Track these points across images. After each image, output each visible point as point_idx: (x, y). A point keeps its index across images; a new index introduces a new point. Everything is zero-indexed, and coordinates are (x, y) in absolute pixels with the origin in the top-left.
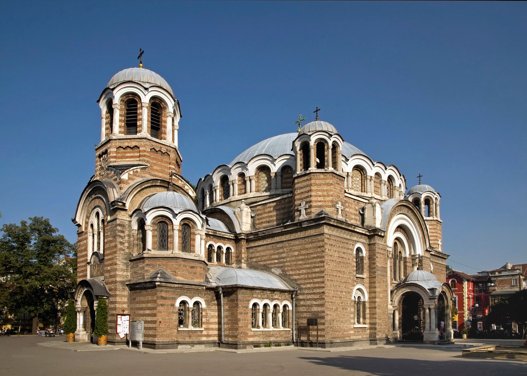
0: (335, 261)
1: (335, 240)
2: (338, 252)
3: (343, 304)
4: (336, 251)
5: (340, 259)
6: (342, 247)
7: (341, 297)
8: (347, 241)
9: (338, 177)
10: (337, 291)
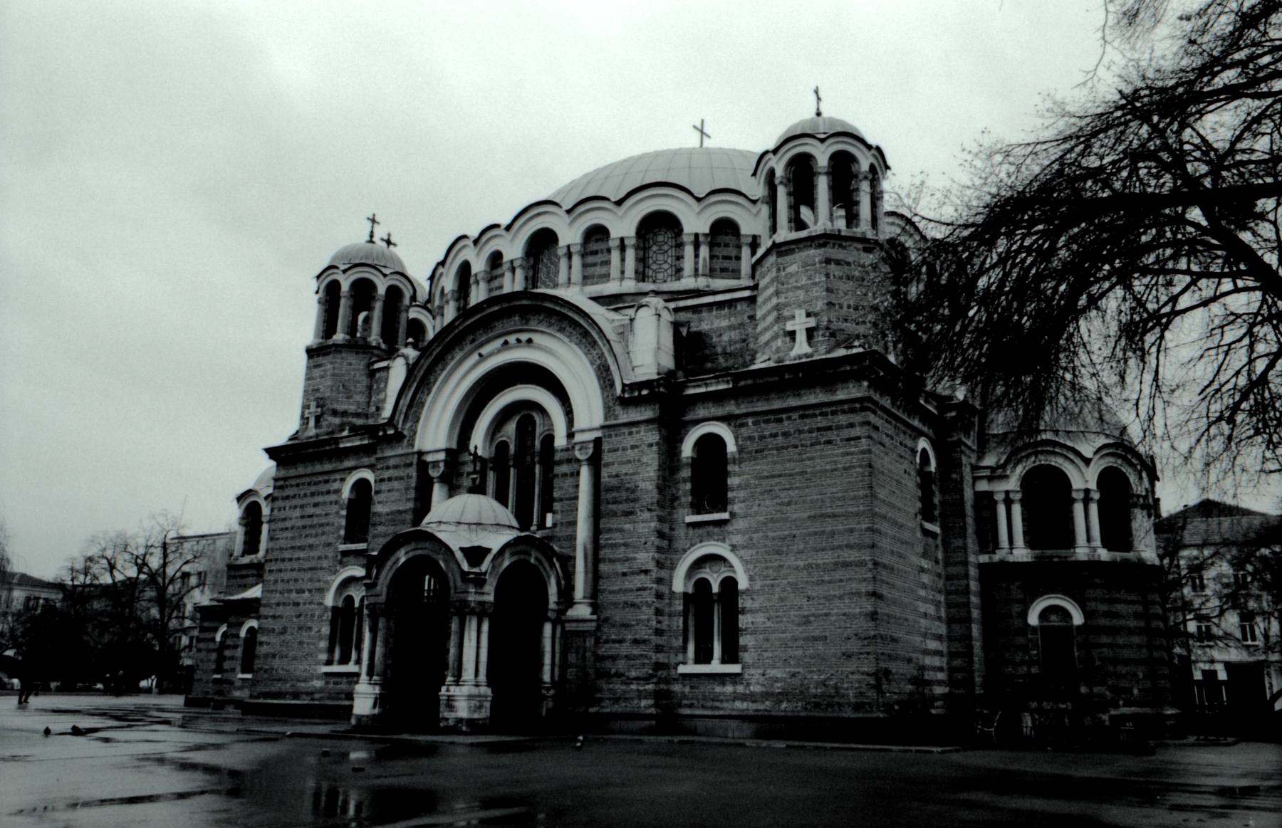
0: (292, 528)
1: (298, 485)
4: (295, 507)
5: (307, 522)
7: (297, 604)
8: (326, 477)
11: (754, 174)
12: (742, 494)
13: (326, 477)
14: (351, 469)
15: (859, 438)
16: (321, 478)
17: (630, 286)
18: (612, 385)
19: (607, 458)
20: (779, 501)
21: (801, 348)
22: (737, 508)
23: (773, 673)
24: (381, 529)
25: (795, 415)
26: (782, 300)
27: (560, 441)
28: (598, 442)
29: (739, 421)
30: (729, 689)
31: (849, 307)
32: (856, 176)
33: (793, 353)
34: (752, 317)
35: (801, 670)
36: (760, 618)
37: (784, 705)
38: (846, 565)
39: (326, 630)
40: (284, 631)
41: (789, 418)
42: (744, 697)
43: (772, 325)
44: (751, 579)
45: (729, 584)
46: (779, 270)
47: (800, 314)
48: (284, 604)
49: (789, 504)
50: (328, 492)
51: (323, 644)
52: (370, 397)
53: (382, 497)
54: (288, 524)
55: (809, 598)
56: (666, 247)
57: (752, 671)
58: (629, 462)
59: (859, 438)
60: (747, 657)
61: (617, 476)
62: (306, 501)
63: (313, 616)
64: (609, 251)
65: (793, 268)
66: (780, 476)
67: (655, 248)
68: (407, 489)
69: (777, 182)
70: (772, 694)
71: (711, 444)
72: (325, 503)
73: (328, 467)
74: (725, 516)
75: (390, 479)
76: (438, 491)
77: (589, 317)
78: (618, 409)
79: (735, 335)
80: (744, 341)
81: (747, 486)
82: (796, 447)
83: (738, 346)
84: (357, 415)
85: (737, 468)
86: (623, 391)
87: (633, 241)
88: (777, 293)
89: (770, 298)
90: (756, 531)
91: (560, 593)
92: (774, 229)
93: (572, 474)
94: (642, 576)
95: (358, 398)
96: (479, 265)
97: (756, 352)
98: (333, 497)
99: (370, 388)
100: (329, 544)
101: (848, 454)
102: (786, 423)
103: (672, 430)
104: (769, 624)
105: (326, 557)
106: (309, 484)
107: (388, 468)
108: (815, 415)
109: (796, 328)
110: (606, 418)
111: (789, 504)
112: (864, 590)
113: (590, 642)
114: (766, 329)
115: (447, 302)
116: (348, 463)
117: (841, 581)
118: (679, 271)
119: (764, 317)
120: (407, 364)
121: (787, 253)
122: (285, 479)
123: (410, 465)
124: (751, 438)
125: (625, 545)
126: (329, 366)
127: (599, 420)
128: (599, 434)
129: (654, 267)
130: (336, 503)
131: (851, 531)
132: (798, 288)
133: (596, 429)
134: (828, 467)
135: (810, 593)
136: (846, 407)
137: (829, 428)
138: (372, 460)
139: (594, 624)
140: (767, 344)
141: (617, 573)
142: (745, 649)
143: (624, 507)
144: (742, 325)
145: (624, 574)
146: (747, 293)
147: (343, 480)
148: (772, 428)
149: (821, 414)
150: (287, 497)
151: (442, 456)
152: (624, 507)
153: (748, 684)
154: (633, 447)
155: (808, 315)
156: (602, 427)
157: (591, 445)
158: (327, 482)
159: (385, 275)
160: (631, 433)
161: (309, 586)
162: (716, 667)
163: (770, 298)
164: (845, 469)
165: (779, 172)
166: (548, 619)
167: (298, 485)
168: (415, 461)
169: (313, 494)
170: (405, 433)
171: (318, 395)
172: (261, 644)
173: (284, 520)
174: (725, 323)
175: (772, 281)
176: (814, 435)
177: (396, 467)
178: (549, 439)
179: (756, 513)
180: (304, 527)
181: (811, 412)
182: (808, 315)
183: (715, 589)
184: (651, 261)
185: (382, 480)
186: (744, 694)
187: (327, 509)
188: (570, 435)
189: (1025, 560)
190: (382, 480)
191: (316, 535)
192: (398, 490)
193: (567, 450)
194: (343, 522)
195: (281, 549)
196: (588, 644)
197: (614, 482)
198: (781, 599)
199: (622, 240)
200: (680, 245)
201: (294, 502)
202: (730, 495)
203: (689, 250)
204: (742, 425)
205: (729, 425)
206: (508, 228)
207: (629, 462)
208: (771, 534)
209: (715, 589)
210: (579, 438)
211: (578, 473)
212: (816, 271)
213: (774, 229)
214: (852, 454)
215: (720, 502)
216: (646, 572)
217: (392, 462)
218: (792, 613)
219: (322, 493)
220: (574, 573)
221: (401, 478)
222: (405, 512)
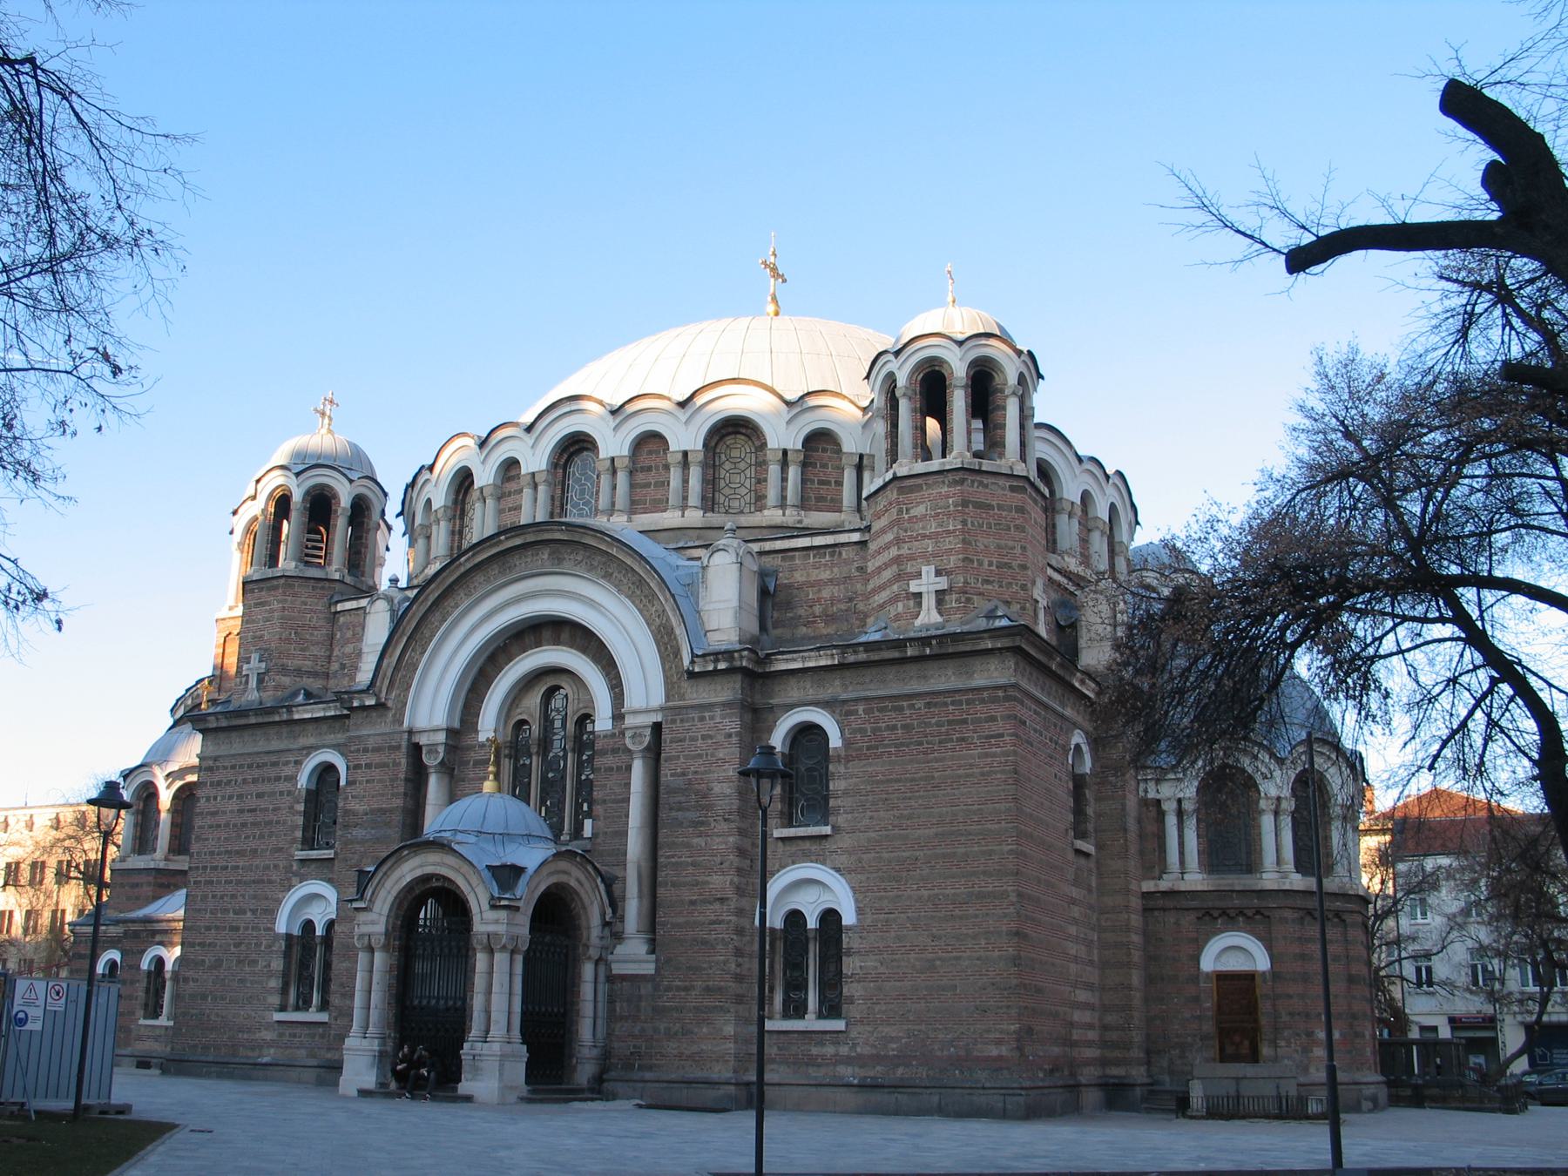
0: (227, 825)
2: (240, 797)
3: (243, 947)
4: (231, 797)
5: (248, 818)
6: (255, 781)
7: (237, 929)
8: (274, 759)
9: (262, 585)
10: (226, 911)
11: (867, 377)
12: (846, 802)
13: (274, 759)
15: (1002, 735)
16: (266, 759)
17: (695, 517)
18: (677, 653)
19: (668, 749)
21: (929, 617)
22: (841, 820)
23: (887, 1030)
24: (358, 833)
25: (919, 704)
26: (905, 551)
27: (603, 722)
28: (657, 727)
30: (830, 1050)
31: (990, 564)
32: (1002, 391)
33: (918, 622)
34: (861, 569)
35: (923, 1027)
37: (900, 1071)
38: (981, 896)
39: (278, 964)
40: (218, 964)
41: (912, 707)
42: (848, 1061)
43: (890, 583)
44: (860, 911)
45: (830, 917)
46: (900, 511)
47: (928, 571)
48: (217, 928)
49: (909, 817)
50: (278, 779)
51: (275, 983)
52: (332, 650)
53: (357, 790)
54: (222, 820)
55: (934, 938)
56: (742, 465)
57: (860, 1028)
58: (700, 756)
59: (1002, 735)
60: (853, 1011)
61: (683, 774)
63: (258, 945)
64: (667, 467)
65: (919, 511)
67: (727, 466)
69: (898, 394)
70: (886, 1056)
71: (808, 733)
72: (272, 794)
73: (276, 745)
74: (827, 830)
76: (434, 787)
77: (648, 563)
78: (686, 684)
79: (838, 591)
80: (851, 600)
82: (921, 744)
83: (843, 607)
84: (315, 674)
85: (842, 769)
86: (692, 662)
87: (701, 457)
88: (898, 541)
89: (887, 547)
90: (868, 851)
91: (606, 924)
92: (893, 455)
93: (619, 769)
94: (717, 906)
95: (316, 651)
96: (484, 477)
97: (866, 616)
98: (283, 786)
99: (332, 637)
100: (280, 850)
101: (987, 755)
102: (907, 712)
103: (756, 717)
104: (882, 970)
105: (276, 866)
106: (250, 766)
107: (366, 750)
108: (946, 704)
109: (923, 589)
110: (668, 698)
111: (909, 817)
112: (1004, 928)
113: (646, 989)
114: (882, 588)
115: (438, 521)
116: (304, 741)
117: (976, 916)
118: (759, 501)
119: (879, 570)
120: (392, 611)
121: (912, 489)
122: (216, 759)
123: (398, 747)
124: (862, 731)
125: (693, 864)
126: (276, 605)
127: (658, 697)
129: (727, 491)
131: (990, 853)
132: (924, 536)
133: (655, 711)
134: (961, 772)
136: (985, 694)
137: (965, 721)
138: (340, 738)
140: (882, 607)
142: (851, 1001)
144: (848, 578)
145: (693, 903)
146: (856, 537)
147: (298, 763)
149: (953, 703)
150: (219, 783)
151: (441, 737)
152: (692, 815)
154: (704, 737)
155: (938, 573)
156: (662, 709)
157: (648, 732)
158: (275, 764)
159: (351, 481)
160: (702, 719)
162: (811, 1023)
163: (887, 547)
164: (983, 774)
165: (902, 381)
166: (589, 958)
167: (233, 767)
168: (404, 744)
169: (255, 781)
170: (390, 704)
171: (261, 644)
172: (186, 980)
173: (214, 814)
174: (826, 575)
175: (891, 525)
177: (377, 750)
178: (585, 718)
179: (867, 829)
180: (244, 825)
181: (941, 699)
182: (938, 573)
183: (812, 923)
184: (722, 484)
185: (357, 767)
186: (848, 1057)
188: (618, 717)
189: (1199, 888)
190: (357, 767)
191: (262, 836)
192: (380, 781)
193: (613, 735)
194: (300, 820)
195: (212, 853)
196: (643, 992)
199: (685, 454)
200: (762, 464)
201: (229, 790)
202: (832, 803)
203: (774, 470)
204: (849, 713)
205: (832, 713)
206: (529, 429)
207: (700, 756)
209: (812, 923)
210: (630, 721)
211: (629, 768)
212: (949, 515)
213: (893, 455)
214: (994, 755)
215: (820, 807)
216: (722, 900)
217: (371, 743)
218: (913, 955)
219: (269, 780)
220: (623, 898)
222: (391, 811)
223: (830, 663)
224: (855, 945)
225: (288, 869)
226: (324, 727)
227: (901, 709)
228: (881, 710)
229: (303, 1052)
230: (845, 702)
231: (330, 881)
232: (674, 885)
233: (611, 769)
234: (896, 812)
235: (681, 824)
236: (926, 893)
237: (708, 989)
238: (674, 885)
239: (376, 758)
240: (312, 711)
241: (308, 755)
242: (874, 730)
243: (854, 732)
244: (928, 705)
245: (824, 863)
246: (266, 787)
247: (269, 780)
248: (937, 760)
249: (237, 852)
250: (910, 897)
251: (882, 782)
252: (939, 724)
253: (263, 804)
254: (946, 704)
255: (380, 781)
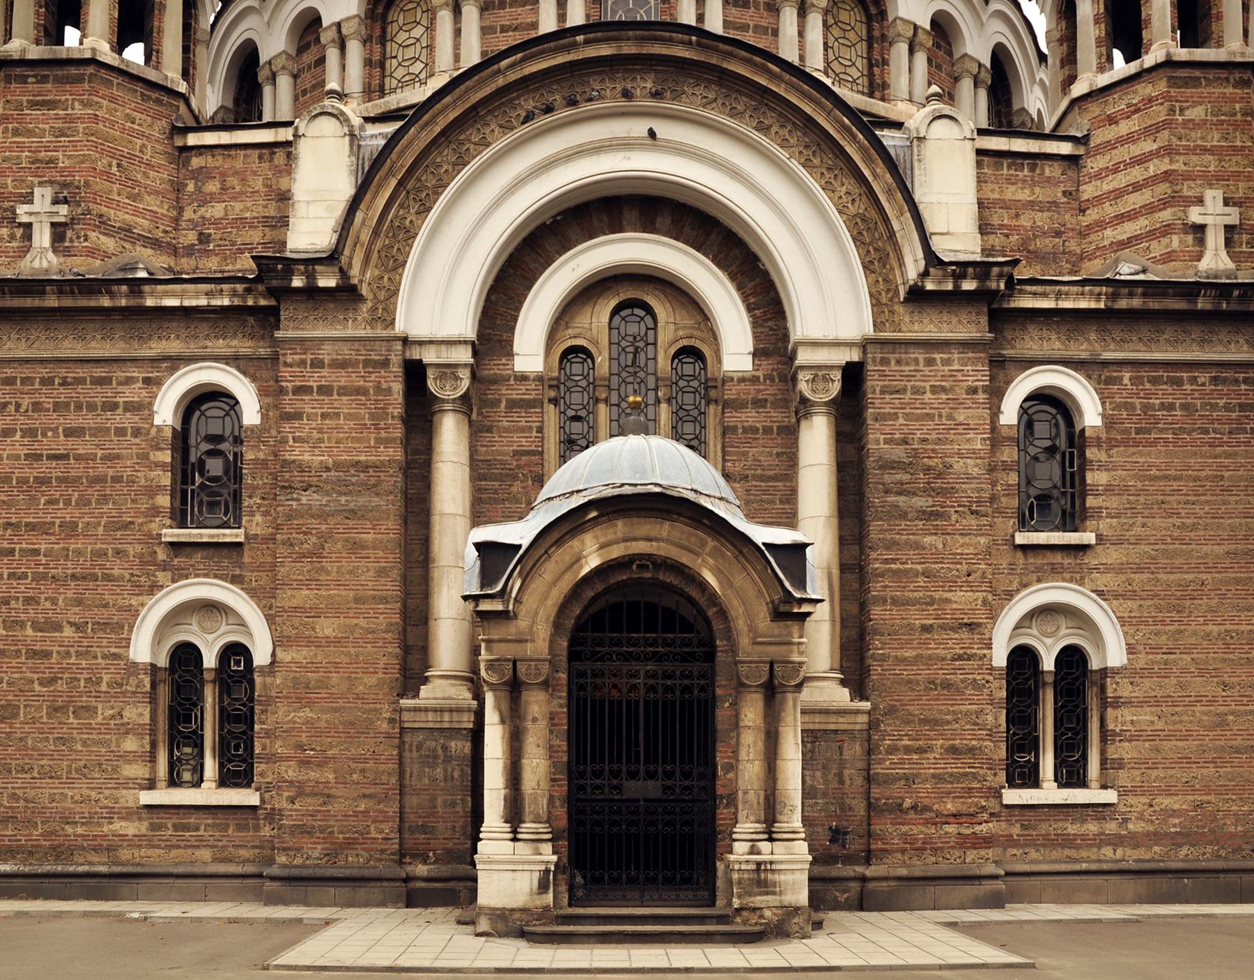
3: (61, 686)
8: (99, 372)
12: (1113, 502)
14: (175, 362)
20: (1178, 522)
23: (1166, 802)
25: (1203, 377)
28: (853, 375)
29: (1106, 374)
36: (1145, 716)
37: (1184, 851)
49: (1194, 527)
58: (930, 417)
62: (38, 421)
66: (1176, 478)
68: (379, 415)
70: (1167, 834)
72: (100, 431)
75: (325, 390)
81: (1125, 490)
82: (1206, 432)
85: (1103, 456)
90: (1139, 569)
94: (964, 634)
104: (1160, 725)
107: (318, 364)
108: (1236, 381)
111: (1194, 527)
128: (855, 356)
130: (137, 432)
135: (1226, 678)
139: (864, 719)
141: (911, 627)
143: (920, 502)
145: (926, 629)
148: (1163, 394)
149: (1245, 381)
153: (1125, 821)
160: (930, 362)
161: (75, 614)
168: (396, 359)
176: (1234, 415)
180: (43, 481)
187: (113, 443)
192: (349, 417)
197: (899, 453)
198: (1182, 686)
204: (1110, 381)
207: (930, 417)
208: (1161, 576)
217: (327, 353)
219: (92, 407)
221: (359, 391)
223: (1093, 305)
224: (1126, 691)
225: (148, 561)
226: (204, 328)
227: (1178, 382)
228: (1155, 381)
229: (206, 854)
230: (1106, 364)
231: (235, 580)
232: (895, 602)
233: (755, 430)
234: (1178, 522)
235: (904, 516)
236: (1216, 628)
237: (953, 750)
238: (895, 602)
239: (342, 379)
240: (181, 295)
241: (173, 369)
242: (1146, 408)
243: (1118, 407)
244: (1215, 380)
245: (1081, 582)
246: (74, 420)
247: (92, 407)
248: (1228, 455)
249: (31, 527)
250: (1195, 633)
251: (1156, 478)
252: (1227, 408)
253: (83, 446)
254: (1236, 381)
255: (349, 417)
